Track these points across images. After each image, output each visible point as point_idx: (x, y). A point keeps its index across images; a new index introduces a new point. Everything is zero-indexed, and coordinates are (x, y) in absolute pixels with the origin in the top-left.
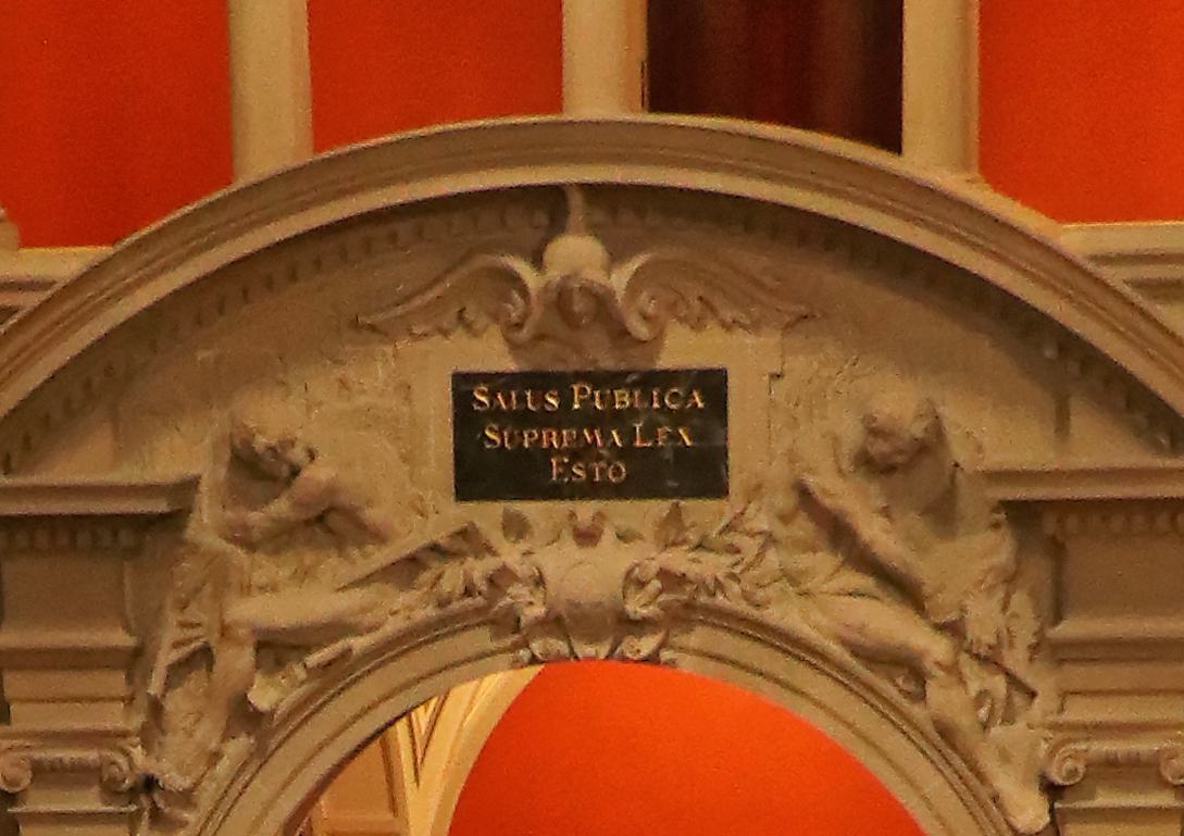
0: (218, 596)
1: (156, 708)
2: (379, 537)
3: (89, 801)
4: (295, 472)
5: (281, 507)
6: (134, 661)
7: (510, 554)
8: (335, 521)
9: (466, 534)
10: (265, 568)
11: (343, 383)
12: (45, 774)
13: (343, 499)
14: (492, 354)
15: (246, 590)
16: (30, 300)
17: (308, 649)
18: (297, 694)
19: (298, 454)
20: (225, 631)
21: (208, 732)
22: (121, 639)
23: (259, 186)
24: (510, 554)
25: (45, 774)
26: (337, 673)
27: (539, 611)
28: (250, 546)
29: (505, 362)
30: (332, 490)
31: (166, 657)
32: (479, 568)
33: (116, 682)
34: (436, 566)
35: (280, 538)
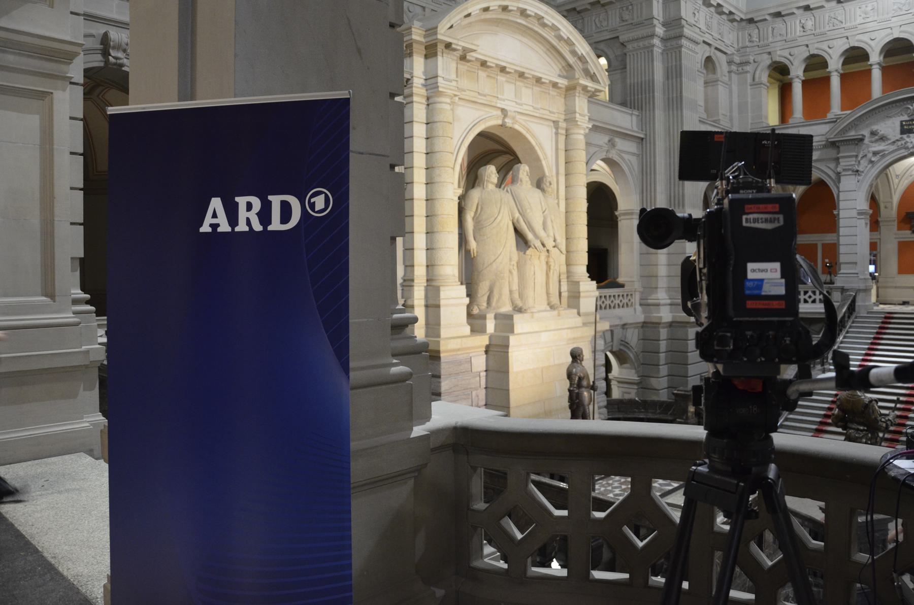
0: (868, 149)
1: (859, 162)
2: (888, 139)
3: (850, 172)
4: (878, 133)
5: (877, 137)
6: (857, 156)
7: (908, 140)
8: (884, 138)
9: (901, 138)
10: (874, 145)
11: (885, 124)
12: (844, 170)
13: (885, 135)
14: (906, 118)
15: (871, 147)
16: (844, 116)
17: (879, 153)
18: (878, 159)
19: (879, 131)
20: (869, 152)
21: (866, 164)
22: (855, 154)
23: (876, 100)
24: (908, 140)
25: (844, 170)
26: (884, 156)
27: (911, 146)
28: (872, 142)
29: (908, 119)
30: (883, 134)
31: (860, 156)
32: (903, 142)
33: (854, 159)
34: (897, 142)
35: (877, 141)
